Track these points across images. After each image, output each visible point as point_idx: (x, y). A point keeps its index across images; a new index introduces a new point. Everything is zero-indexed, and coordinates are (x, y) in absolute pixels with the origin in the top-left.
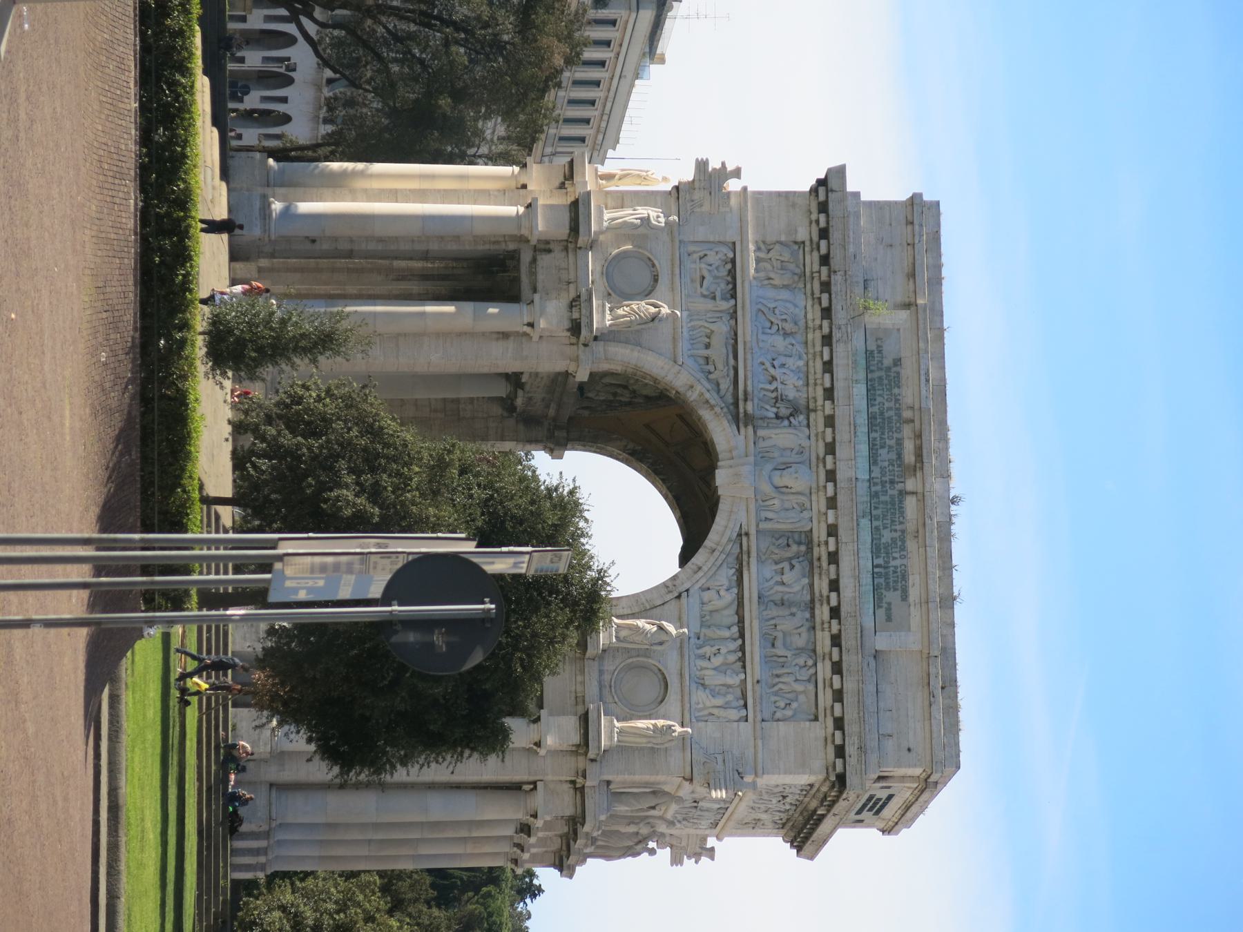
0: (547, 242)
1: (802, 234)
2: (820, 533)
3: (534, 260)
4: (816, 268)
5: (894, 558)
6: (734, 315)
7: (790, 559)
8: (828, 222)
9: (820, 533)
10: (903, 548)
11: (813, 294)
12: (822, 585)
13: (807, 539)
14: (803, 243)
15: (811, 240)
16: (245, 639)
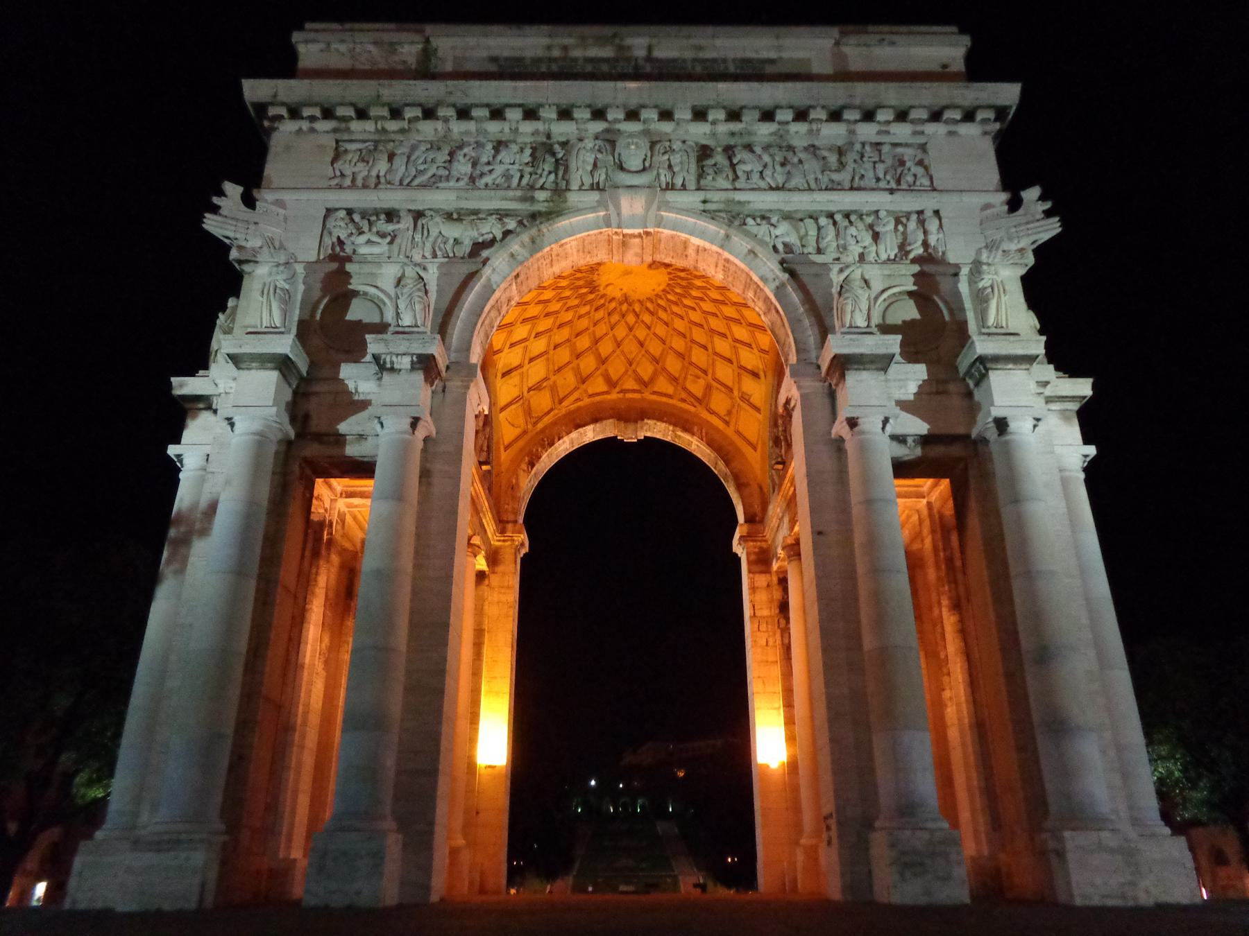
0: (293, 420)
1: (329, 141)
2: (699, 132)
3: (319, 437)
4: (369, 126)
5: (727, 68)
6: (418, 215)
7: (733, 166)
8: (316, 105)
9: (699, 132)
10: (714, 60)
11: (402, 131)
12: (765, 131)
13: (704, 152)
14: (337, 141)
15: (335, 131)
16: (946, 879)
